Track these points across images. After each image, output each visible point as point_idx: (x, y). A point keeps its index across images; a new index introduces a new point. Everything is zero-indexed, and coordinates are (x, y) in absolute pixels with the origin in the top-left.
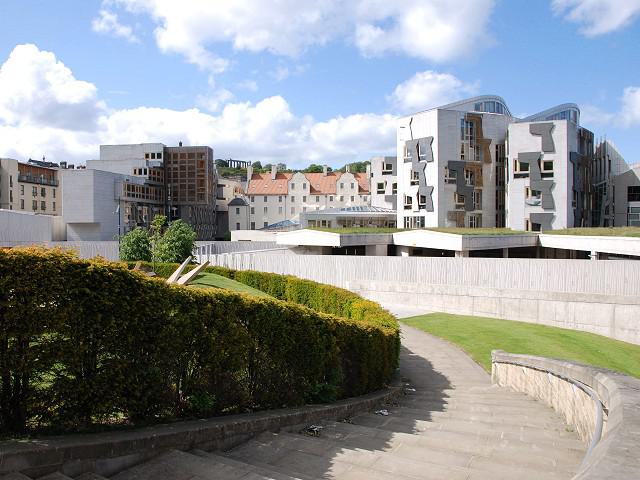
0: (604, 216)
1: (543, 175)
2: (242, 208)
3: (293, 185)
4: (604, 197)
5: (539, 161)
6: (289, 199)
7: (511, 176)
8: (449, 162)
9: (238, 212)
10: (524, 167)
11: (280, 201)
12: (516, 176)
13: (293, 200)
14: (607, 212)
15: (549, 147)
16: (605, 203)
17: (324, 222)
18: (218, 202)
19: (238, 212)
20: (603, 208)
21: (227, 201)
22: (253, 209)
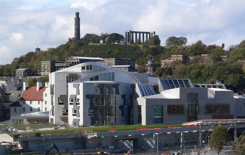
0: (132, 118)
1: (77, 104)
2: (18, 108)
3: (46, 95)
4: (132, 109)
5: (76, 97)
6: (44, 102)
7: (69, 104)
8: (61, 95)
9: (15, 111)
10: (72, 101)
11: (39, 103)
12: (70, 104)
13: (46, 103)
14: (133, 117)
15: (78, 93)
16: (132, 113)
17: (20, 120)
18: (5, 104)
19: (15, 111)
20: (131, 114)
21: (11, 104)
22: (24, 108)
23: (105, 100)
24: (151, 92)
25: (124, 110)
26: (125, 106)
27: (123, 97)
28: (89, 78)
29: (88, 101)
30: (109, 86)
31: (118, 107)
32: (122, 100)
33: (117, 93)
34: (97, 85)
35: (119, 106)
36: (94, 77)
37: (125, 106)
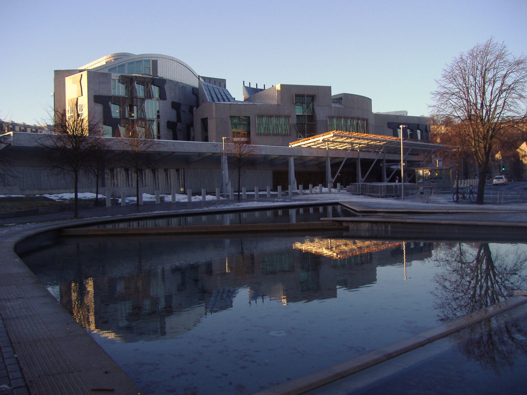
4: (192, 129)
16: (192, 135)
23: (135, 108)
24: (227, 97)
25: (178, 132)
26: (178, 124)
27: (176, 106)
28: (107, 69)
29: (99, 108)
30: (143, 81)
31: (163, 124)
32: (174, 112)
33: (162, 96)
34: (118, 78)
35: (166, 121)
36: (115, 68)
37: (178, 124)
